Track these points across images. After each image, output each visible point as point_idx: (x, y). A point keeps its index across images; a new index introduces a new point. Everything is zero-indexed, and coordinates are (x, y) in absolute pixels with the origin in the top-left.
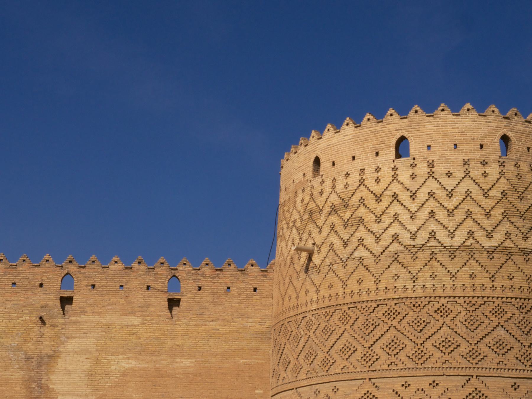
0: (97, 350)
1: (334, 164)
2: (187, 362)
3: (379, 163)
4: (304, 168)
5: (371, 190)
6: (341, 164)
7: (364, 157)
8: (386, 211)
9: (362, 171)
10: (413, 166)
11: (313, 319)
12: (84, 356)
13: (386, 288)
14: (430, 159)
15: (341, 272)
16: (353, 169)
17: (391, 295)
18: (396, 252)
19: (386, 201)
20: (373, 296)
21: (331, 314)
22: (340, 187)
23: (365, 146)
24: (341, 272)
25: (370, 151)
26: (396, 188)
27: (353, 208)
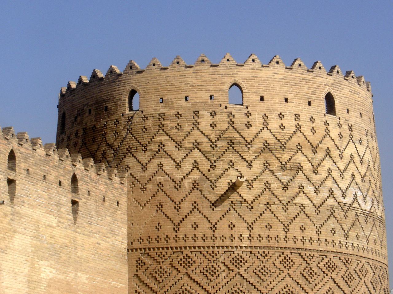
0: (32, 252)
1: (262, 99)
2: (83, 278)
3: (312, 113)
4: (211, 89)
5: (308, 139)
6: (272, 102)
7: (297, 102)
8: (322, 164)
9: (297, 116)
10: (340, 126)
11: (244, 256)
12: (24, 257)
13: (326, 240)
14: (350, 123)
15: (282, 215)
16: (288, 112)
17: (330, 248)
18: (332, 207)
19: (320, 155)
20: (315, 246)
21: (271, 255)
22: (274, 124)
23: (298, 91)
24: (282, 215)
25: (303, 99)
26: (328, 143)
27: (290, 151)
